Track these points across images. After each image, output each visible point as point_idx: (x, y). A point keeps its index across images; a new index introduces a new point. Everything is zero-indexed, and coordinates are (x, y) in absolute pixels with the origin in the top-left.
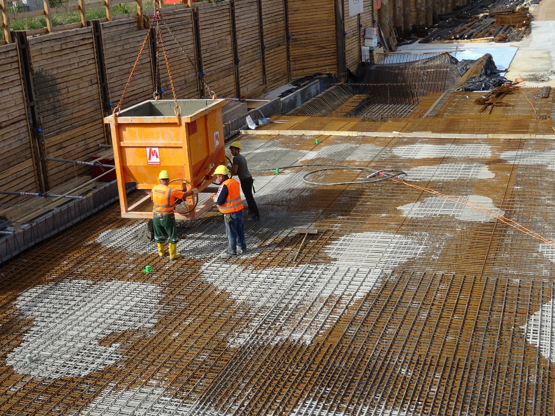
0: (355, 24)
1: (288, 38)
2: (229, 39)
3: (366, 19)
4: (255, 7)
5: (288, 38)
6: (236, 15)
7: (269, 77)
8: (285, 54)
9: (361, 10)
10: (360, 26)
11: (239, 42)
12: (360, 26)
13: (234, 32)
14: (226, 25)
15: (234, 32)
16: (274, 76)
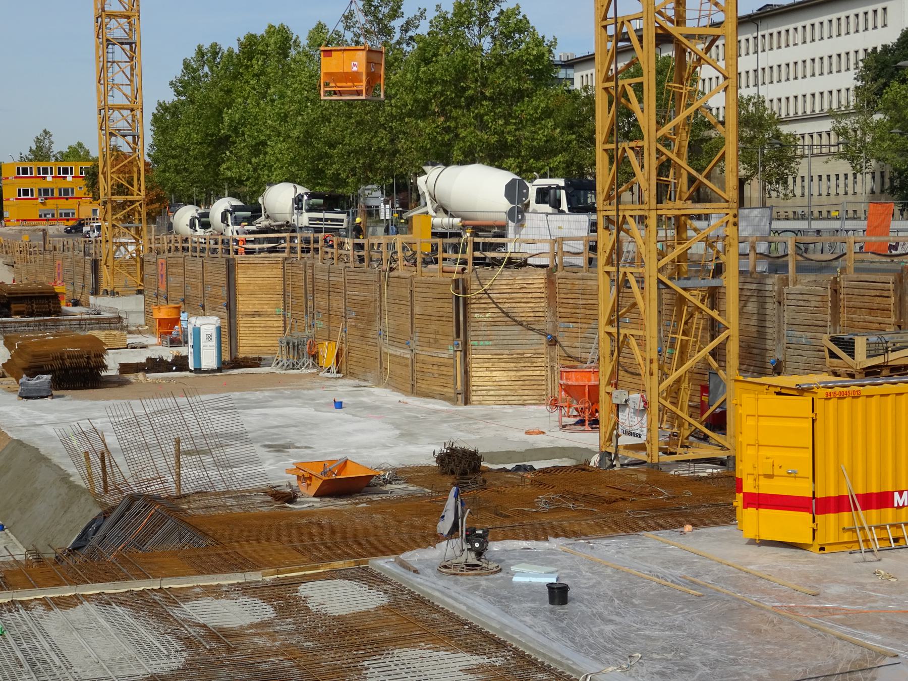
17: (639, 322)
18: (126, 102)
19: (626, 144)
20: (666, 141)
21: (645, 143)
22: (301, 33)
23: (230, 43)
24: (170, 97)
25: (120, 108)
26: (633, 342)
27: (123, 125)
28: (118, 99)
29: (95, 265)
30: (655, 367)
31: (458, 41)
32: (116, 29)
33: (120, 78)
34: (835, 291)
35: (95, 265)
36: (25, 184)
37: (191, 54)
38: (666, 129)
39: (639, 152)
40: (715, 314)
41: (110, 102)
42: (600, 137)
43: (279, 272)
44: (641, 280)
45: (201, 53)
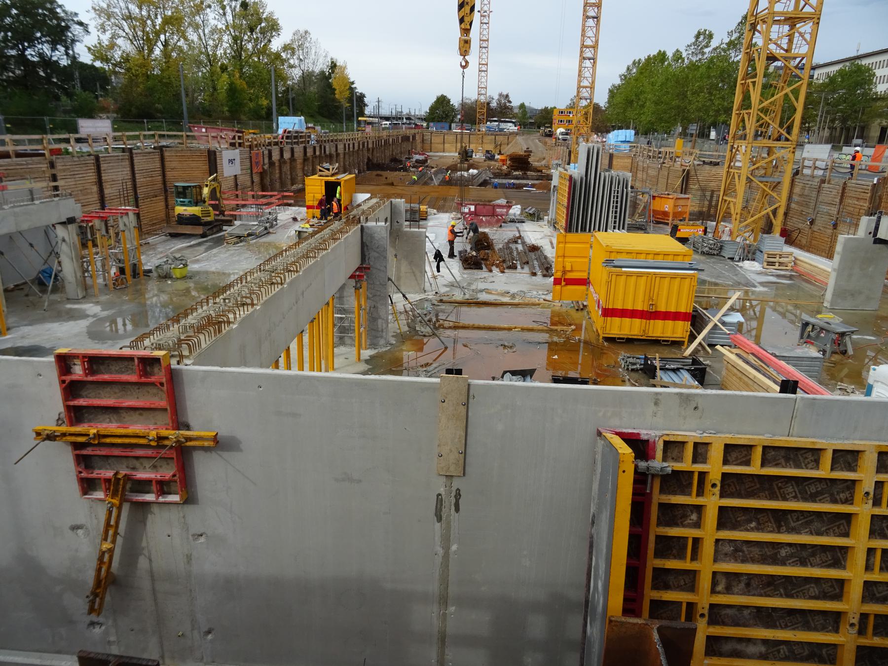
0: (232, 183)
1: (166, 191)
2: (95, 189)
3: (245, 180)
4: (127, 163)
5: (166, 191)
6: (102, 169)
7: (144, 222)
8: (163, 203)
9: (239, 172)
10: (237, 185)
11: (106, 191)
12: (237, 185)
13: (100, 183)
14: (92, 176)
15: (100, 183)
16: (150, 221)
17: (736, 197)
18: (589, 85)
19: (745, 111)
20: (765, 111)
21: (751, 111)
22: (670, 54)
23: (643, 57)
24: (618, 82)
25: (586, 87)
26: (732, 205)
27: (586, 95)
28: (585, 83)
29: (570, 152)
30: (738, 216)
31: (726, 59)
32: (588, 53)
33: (587, 74)
34: (844, 189)
35: (570, 152)
36: (562, 118)
37: (630, 63)
38: (766, 103)
39: (749, 114)
40: (774, 195)
41: (582, 84)
42: (735, 108)
43: (630, 161)
44: (739, 176)
45: (634, 63)
